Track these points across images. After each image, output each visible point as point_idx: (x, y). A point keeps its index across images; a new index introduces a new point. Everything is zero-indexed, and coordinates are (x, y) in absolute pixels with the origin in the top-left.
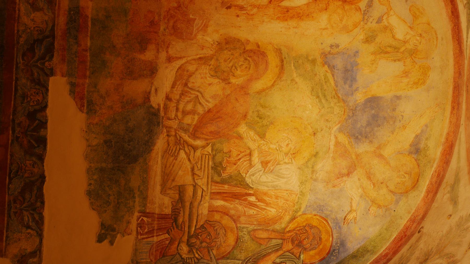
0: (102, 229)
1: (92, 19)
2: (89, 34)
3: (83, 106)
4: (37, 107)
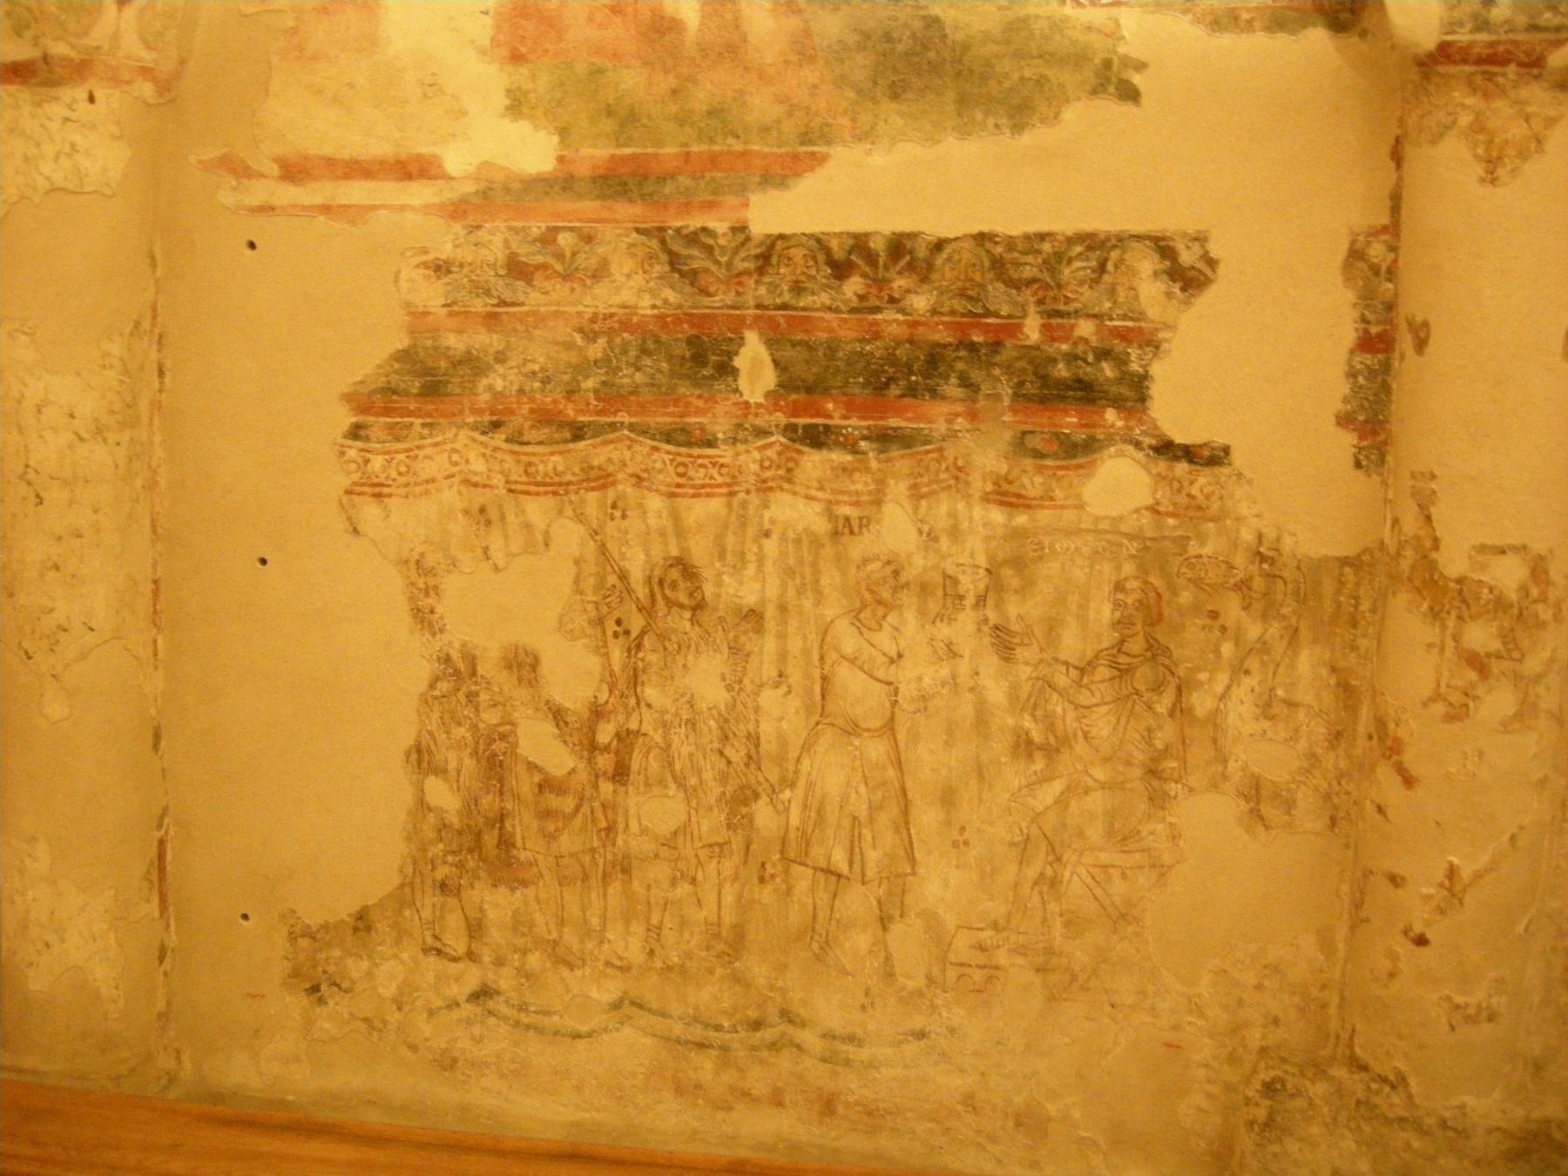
0: (1105, 91)
1: (618, 146)
2: (650, 150)
3: (814, 154)
4: (821, 258)
